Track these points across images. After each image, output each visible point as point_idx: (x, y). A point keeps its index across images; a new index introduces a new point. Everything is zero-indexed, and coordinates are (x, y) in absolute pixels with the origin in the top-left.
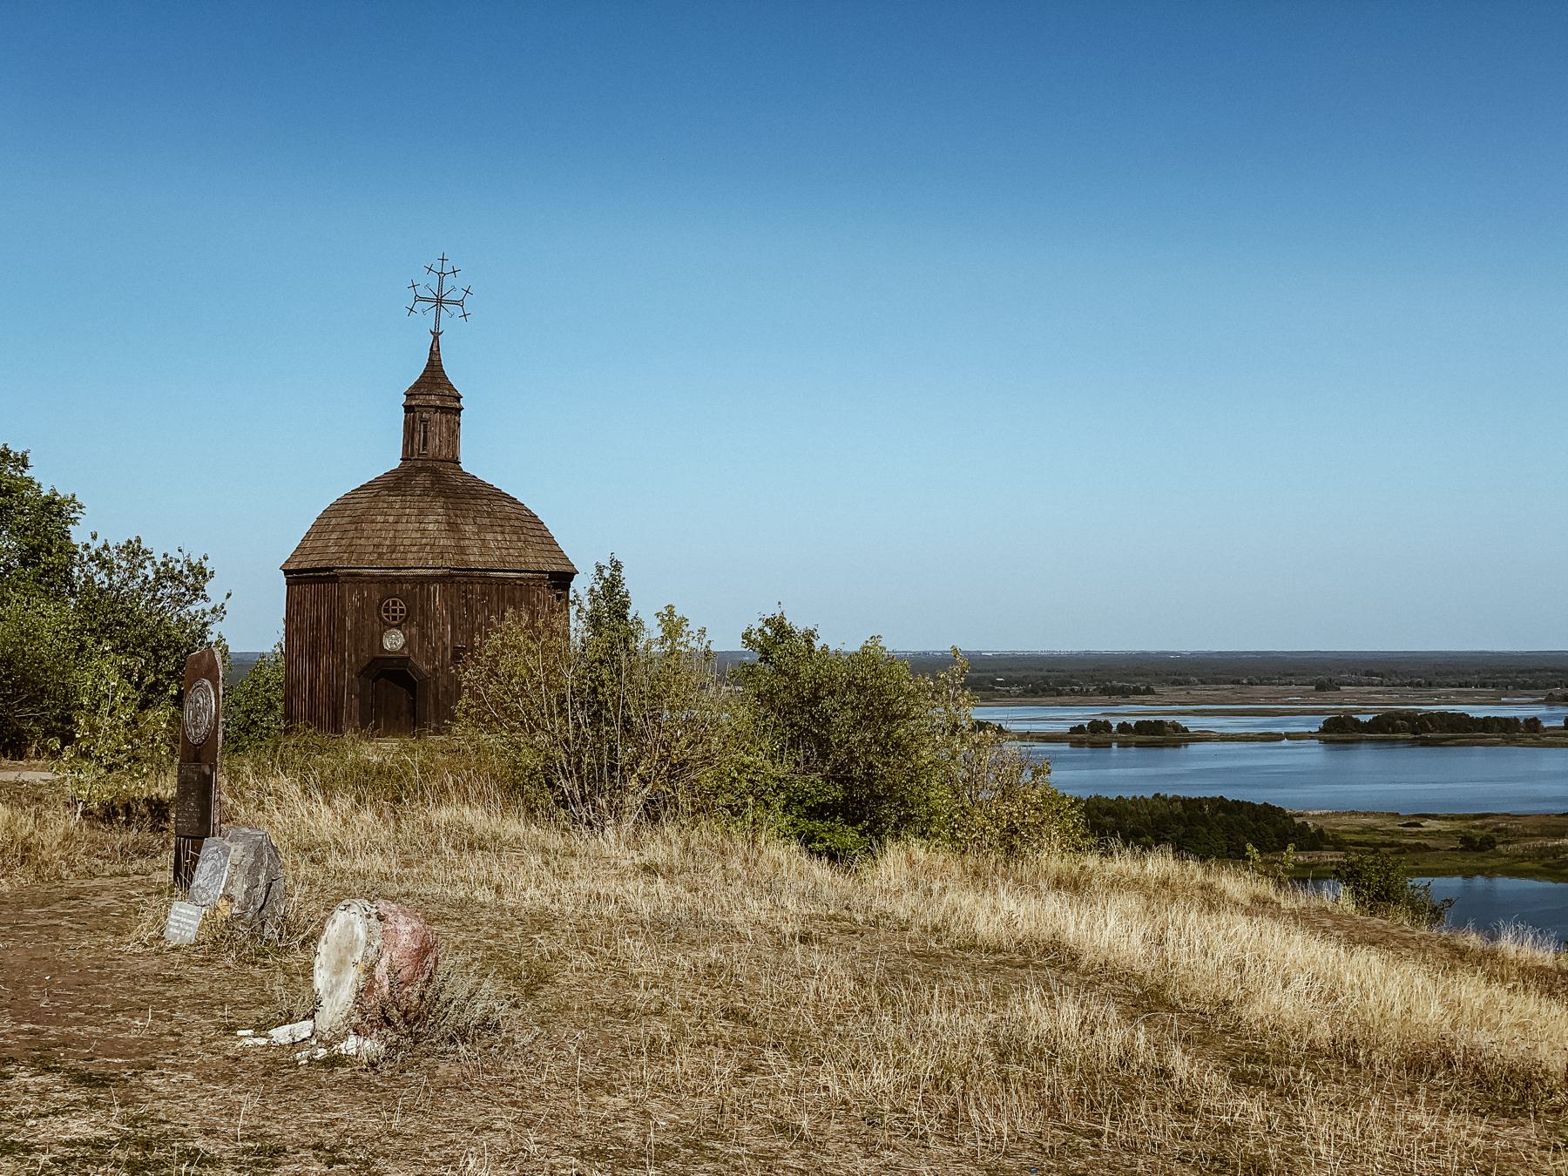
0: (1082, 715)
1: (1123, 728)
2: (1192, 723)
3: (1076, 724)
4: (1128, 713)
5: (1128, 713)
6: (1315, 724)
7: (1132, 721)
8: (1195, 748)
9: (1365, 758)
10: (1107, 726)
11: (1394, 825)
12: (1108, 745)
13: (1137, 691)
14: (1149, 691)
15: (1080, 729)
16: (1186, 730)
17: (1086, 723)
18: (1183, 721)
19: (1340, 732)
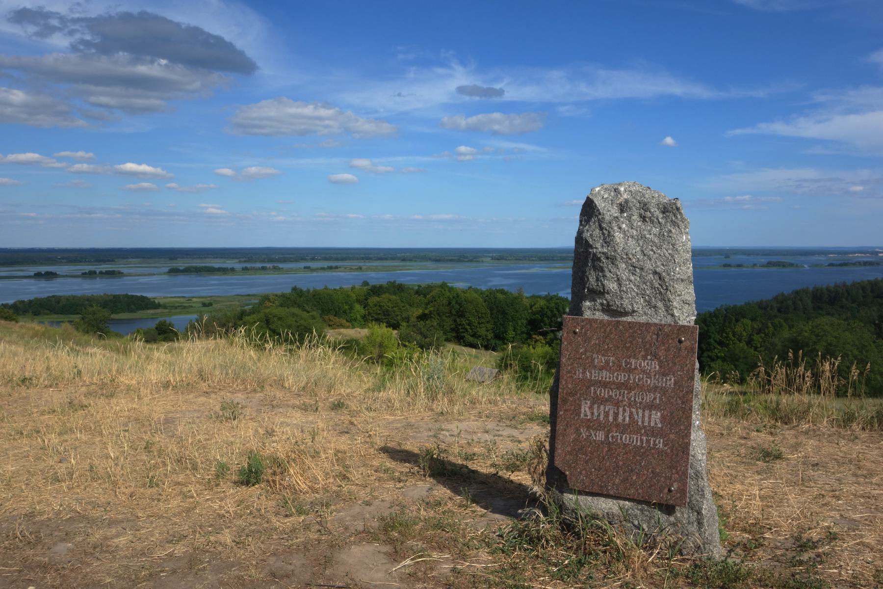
0: (87, 268)
1: (101, 273)
2: (125, 271)
3: (84, 271)
4: (105, 267)
5: (105, 267)
6: (166, 270)
7: (104, 271)
8: (125, 278)
9: (182, 278)
10: (95, 273)
11: (182, 300)
12: (95, 278)
13: (109, 261)
14: (113, 261)
15: (83, 274)
16: (123, 273)
17: (87, 272)
18: (122, 270)
19: (174, 271)
